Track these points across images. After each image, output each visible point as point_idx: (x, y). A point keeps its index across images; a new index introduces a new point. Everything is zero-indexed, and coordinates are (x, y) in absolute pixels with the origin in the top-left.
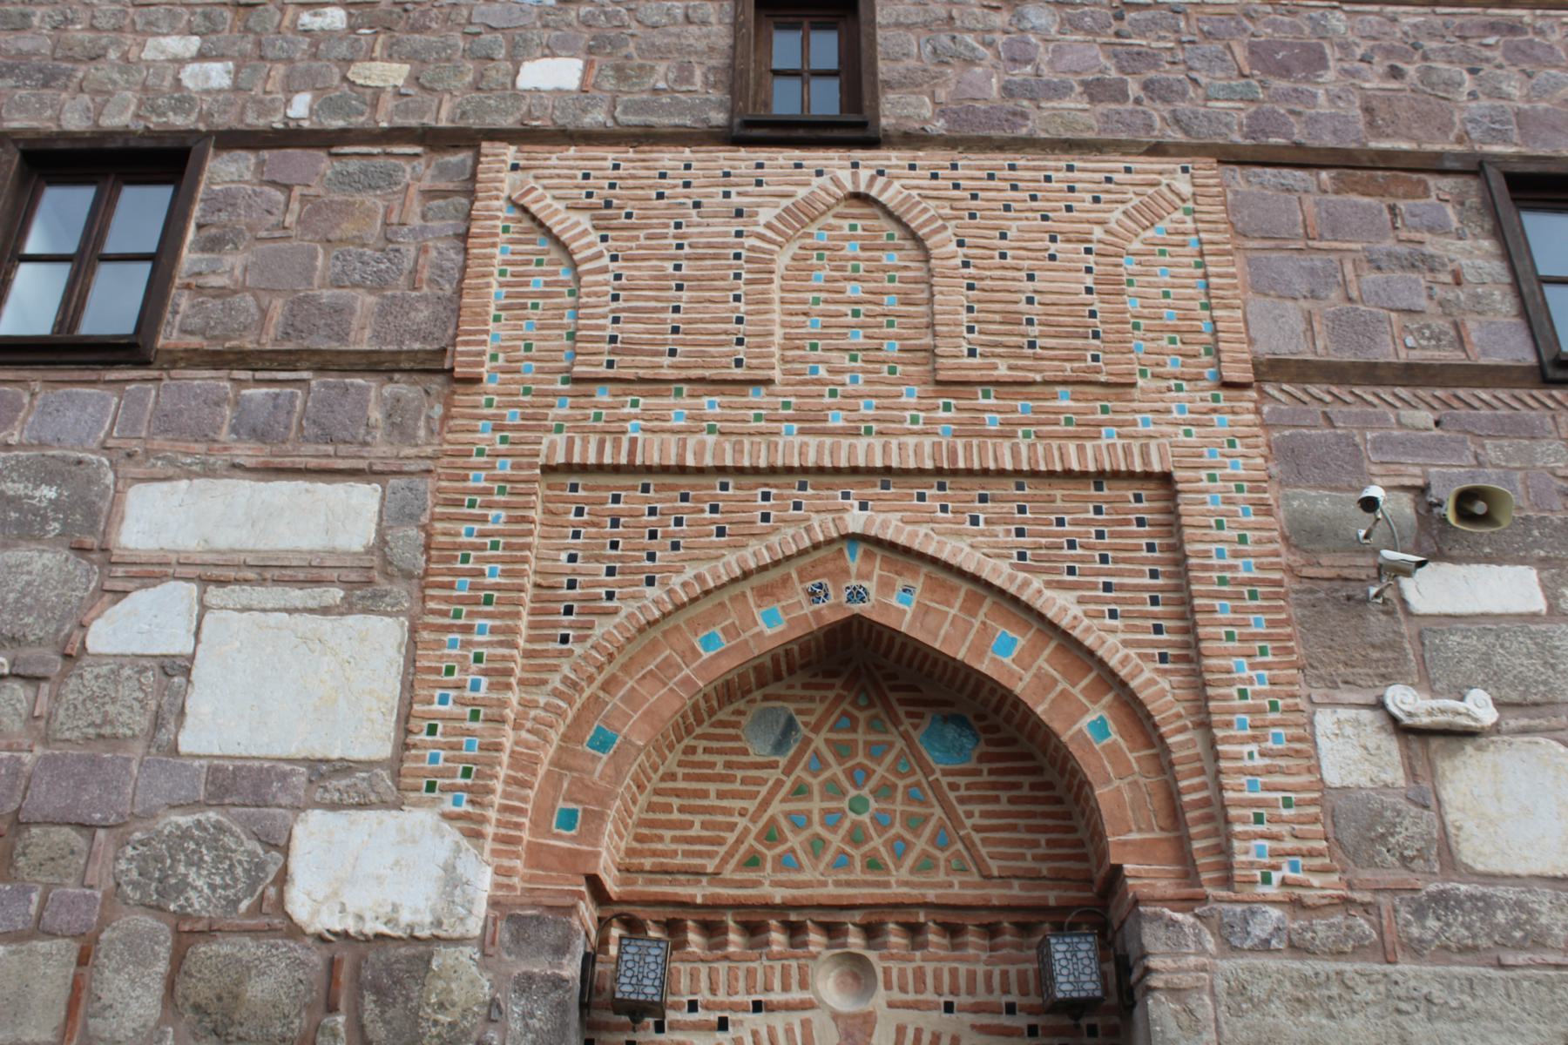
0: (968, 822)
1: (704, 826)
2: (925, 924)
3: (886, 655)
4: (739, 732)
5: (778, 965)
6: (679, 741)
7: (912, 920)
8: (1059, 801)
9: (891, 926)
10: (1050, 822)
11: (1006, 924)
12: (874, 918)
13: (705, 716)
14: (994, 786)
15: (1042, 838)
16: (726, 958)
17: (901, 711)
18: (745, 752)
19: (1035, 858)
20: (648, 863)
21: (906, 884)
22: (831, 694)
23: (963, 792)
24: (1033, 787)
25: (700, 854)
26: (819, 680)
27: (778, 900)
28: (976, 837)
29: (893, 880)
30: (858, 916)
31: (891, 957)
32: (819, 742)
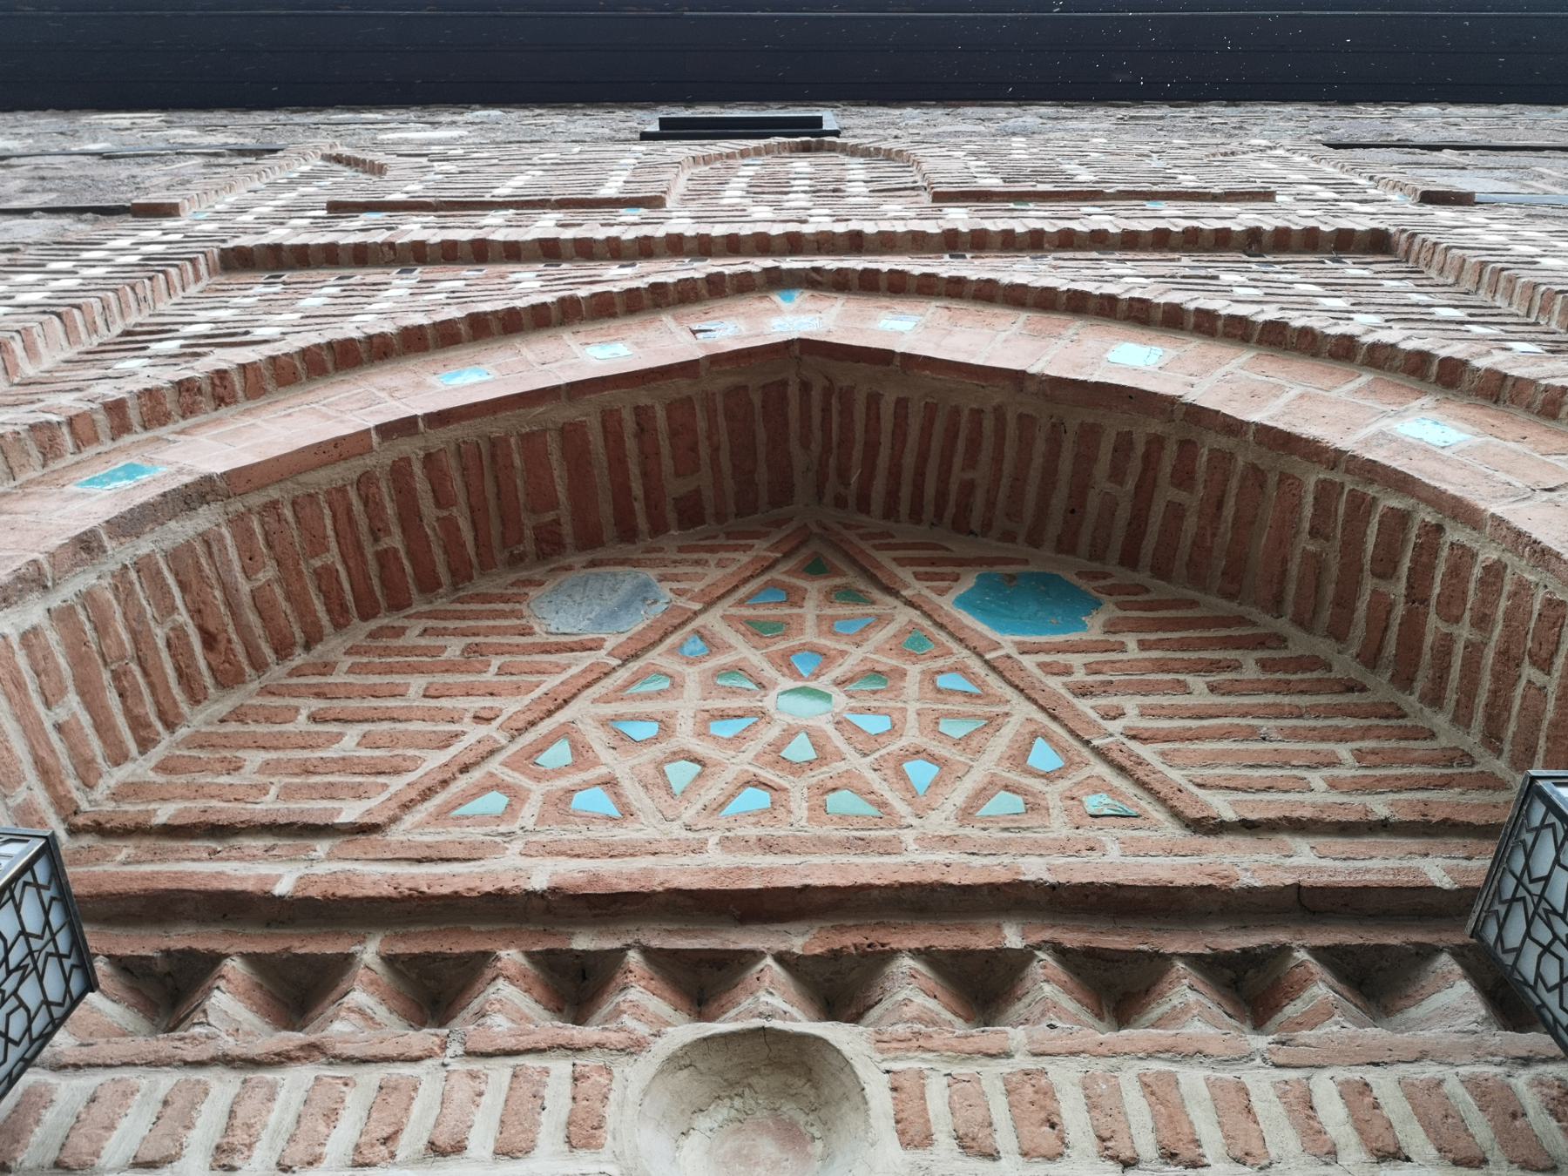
0: (1115, 726)
1: (366, 741)
2: (1024, 958)
3: (864, 504)
4: (523, 607)
5: (499, 1073)
6: (365, 617)
7: (981, 941)
8: (1350, 687)
9: (906, 963)
10: (1350, 723)
11: (1302, 955)
12: (850, 939)
13: (444, 577)
14: (1162, 667)
15: (1344, 751)
16: (313, 1051)
17: (905, 574)
18: (526, 631)
19: (1333, 785)
20: (164, 813)
21: (951, 841)
22: (744, 558)
23: (1080, 676)
24: (1264, 665)
25: (330, 792)
26: (722, 541)
27: (539, 882)
28: (1145, 751)
29: (908, 836)
30: (800, 941)
31: (917, 1042)
32: (712, 620)
